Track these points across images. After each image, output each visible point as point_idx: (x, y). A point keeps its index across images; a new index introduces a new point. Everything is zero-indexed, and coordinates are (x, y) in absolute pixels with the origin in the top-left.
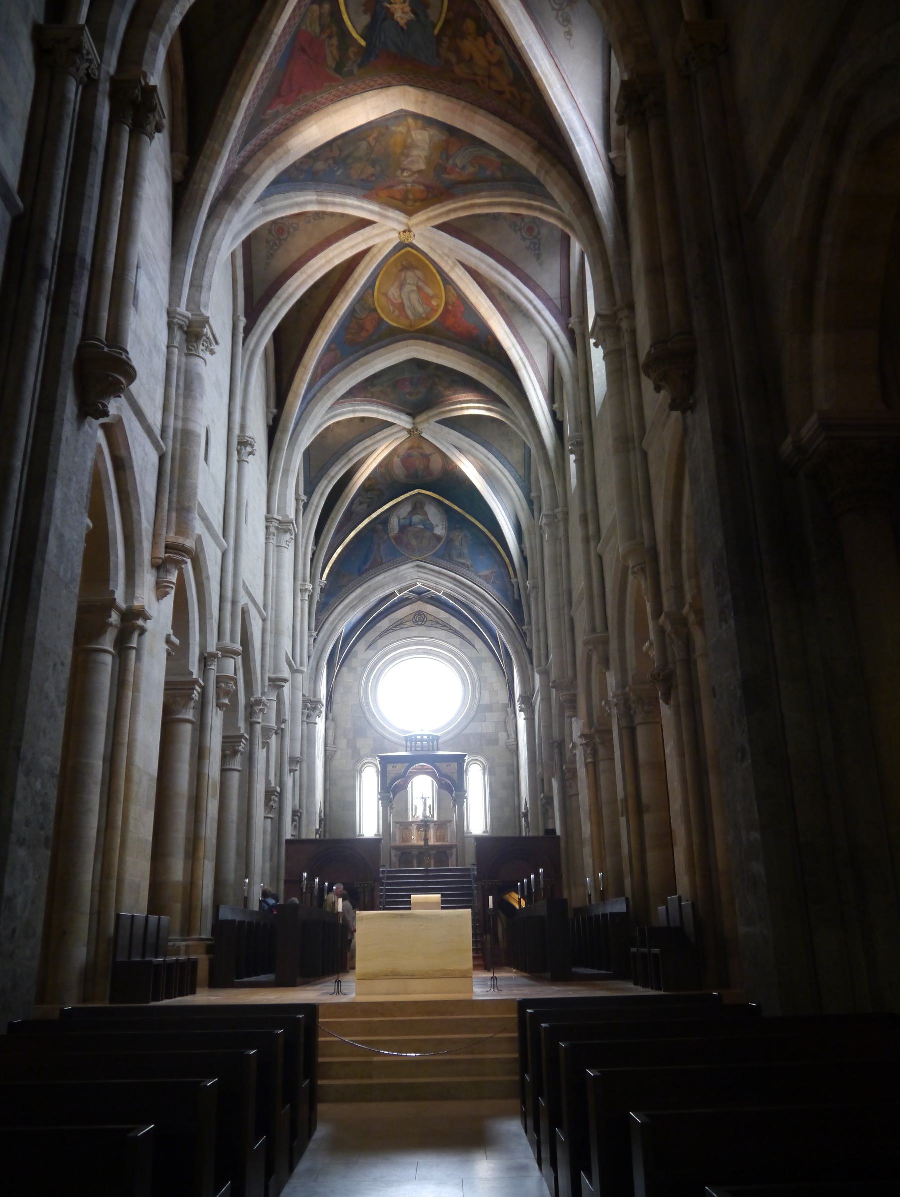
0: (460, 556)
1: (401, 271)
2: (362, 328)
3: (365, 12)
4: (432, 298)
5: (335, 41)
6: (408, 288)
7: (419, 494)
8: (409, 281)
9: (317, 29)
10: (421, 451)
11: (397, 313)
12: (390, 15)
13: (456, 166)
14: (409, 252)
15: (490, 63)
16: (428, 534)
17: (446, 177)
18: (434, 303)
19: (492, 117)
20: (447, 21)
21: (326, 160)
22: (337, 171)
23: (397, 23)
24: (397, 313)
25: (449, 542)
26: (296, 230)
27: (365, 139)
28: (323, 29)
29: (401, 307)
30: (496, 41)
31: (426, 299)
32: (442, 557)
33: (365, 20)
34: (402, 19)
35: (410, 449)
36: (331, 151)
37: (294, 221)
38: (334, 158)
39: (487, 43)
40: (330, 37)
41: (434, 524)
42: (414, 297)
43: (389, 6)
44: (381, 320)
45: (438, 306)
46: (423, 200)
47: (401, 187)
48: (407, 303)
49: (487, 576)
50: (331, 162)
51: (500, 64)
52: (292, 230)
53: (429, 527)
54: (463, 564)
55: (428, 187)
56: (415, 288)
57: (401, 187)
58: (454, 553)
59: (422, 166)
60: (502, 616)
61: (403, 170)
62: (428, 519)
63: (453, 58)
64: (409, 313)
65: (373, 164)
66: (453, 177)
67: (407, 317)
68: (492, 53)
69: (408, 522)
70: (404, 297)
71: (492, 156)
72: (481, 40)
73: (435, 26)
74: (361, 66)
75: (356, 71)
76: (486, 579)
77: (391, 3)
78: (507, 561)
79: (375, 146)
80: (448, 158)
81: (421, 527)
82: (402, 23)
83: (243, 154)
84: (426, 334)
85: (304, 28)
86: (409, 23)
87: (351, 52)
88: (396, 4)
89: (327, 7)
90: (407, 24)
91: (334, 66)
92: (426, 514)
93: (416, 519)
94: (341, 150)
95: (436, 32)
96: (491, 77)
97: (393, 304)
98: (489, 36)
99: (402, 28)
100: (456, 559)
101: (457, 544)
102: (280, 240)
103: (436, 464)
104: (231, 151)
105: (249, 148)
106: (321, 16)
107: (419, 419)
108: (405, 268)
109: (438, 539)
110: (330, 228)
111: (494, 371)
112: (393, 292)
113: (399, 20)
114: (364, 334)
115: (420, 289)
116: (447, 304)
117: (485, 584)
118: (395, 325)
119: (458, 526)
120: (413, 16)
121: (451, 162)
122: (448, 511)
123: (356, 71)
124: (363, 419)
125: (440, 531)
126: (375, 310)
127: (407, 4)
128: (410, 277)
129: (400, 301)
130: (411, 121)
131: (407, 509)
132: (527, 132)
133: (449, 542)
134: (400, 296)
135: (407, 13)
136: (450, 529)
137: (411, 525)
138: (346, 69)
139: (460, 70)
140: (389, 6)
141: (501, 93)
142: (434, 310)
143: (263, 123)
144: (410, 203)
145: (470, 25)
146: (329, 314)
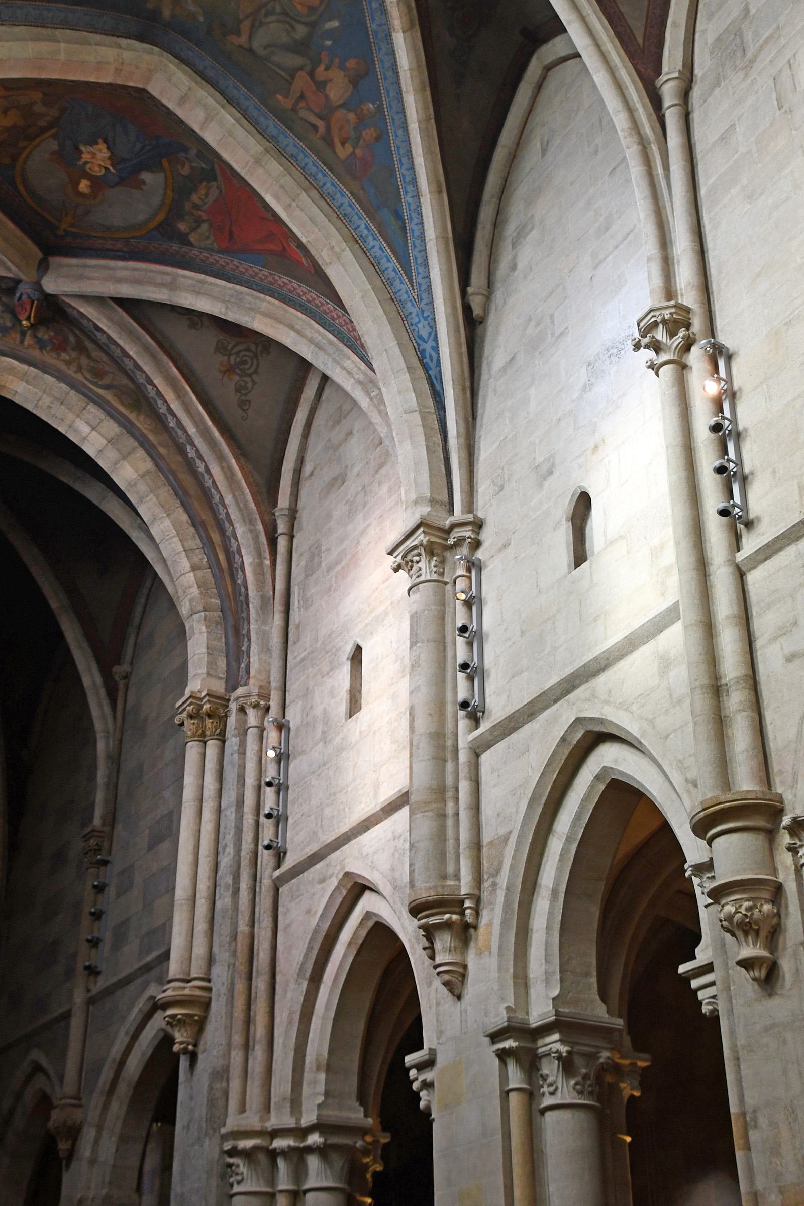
3: (143, 182)
9: (204, 227)
21: (321, 86)
22: (330, 33)
23: (108, 148)
27: (251, 50)
28: (199, 222)
34: (100, 150)
36: (302, 97)
38: (311, 74)
40: (196, 207)
43: (111, 168)
74: (186, 150)
75: (193, 152)
77: (106, 169)
79: (248, 16)
82: (102, 146)
86: (93, 143)
88: (100, 166)
90: (97, 143)
91: (214, 184)
94: (293, 73)
95: (54, 131)
99: (105, 141)
104: (342, 342)
113: (105, 150)
120: (83, 148)
123: (193, 152)
135: (89, 153)
138: (204, 166)
140: (111, 168)
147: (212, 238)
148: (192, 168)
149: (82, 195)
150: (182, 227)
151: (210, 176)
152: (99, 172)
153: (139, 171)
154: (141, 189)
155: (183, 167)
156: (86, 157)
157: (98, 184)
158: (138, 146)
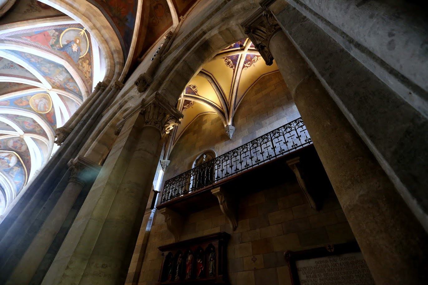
0: (12, 174)
1: (43, 98)
2: (21, 103)
3: (66, 42)
4: (47, 108)
5: (55, 40)
6: (41, 102)
7: (13, 153)
8: (43, 101)
9: (52, 35)
10: (22, 143)
11: (35, 106)
12: (71, 47)
13: (69, 85)
14: (47, 95)
15: (87, 71)
16: (7, 164)
17: (66, 85)
18: (47, 110)
19: (81, 80)
20: (83, 57)
24: (35, 106)
25: (12, 168)
26: (17, 69)
28: (53, 36)
29: (37, 105)
30: (91, 67)
31: (45, 107)
32: (6, 172)
33: (66, 43)
35: (18, 140)
37: (17, 66)
39: (89, 67)
40: (54, 39)
41: (11, 162)
42: (42, 106)
44: (29, 104)
45: (48, 111)
46: (58, 87)
47: (54, 81)
48: (39, 105)
49: (16, 182)
50: (37, 62)
51: (89, 72)
52: (16, 68)
53: (9, 162)
54: (11, 176)
55: (61, 85)
56: (44, 103)
57: (54, 81)
58: (11, 172)
59: (62, 80)
60: (12, 195)
61: (57, 78)
62: (10, 160)
63: (80, 65)
64: (38, 108)
65: (49, 70)
66: (67, 87)
67: (37, 108)
68: (89, 69)
69: (3, 158)
70: (39, 103)
71: (78, 88)
72: (88, 65)
73: (80, 56)
76: (16, 183)
78: (26, 181)
80: (68, 82)
81: (6, 161)
82: (74, 50)
83: (7, 38)
84: (40, 115)
85: (48, 32)
86: (75, 51)
87: (57, 46)
89: (57, 33)
91: (51, 44)
92: (11, 158)
93: (6, 158)
95: (80, 57)
96: (86, 73)
97: (35, 103)
98: (90, 66)
99: (73, 51)
100: (10, 174)
101: (14, 170)
102: (10, 67)
103: (23, 149)
105: (10, 39)
106: (54, 33)
107: (26, 134)
108: (44, 98)
109: (9, 166)
110: (27, 75)
111: (52, 133)
112: (37, 101)
114: (21, 104)
115: (45, 104)
116: (50, 112)
117: (14, 184)
118: (33, 108)
119: (18, 166)
120: (77, 51)
121: (69, 83)
122: (19, 161)
123: (56, 49)
124: (8, 125)
125: (12, 165)
126: (29, 101)
127: (77, 48)
128: (44, 100)
129: (38, 104)
130: (64, 69)
131: (6, 154)
132: (87, 88)
133: (12, 168)
134: (39, 103)
136: (15, 166)
137: (3, 159)
139: (80, 67)
141: (86, 77)
142: (45, 111)
143: (20, 38)
144: (54, 85)
145: (87, 61)
146: (13, 93)
147: (49, 33)
148: (56, 46)
149: (79, 39)
150: (57, 33)
151: (52, 46)
152: (75, 44)
153: (67, 45)
154: (67, 40)
155: (58, 47)
156: (77, 49)
157: (75, 42)
158: (67, 49)
